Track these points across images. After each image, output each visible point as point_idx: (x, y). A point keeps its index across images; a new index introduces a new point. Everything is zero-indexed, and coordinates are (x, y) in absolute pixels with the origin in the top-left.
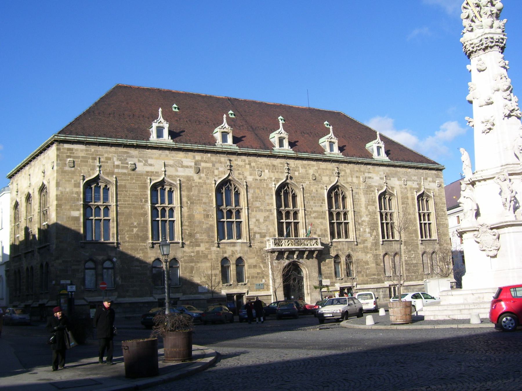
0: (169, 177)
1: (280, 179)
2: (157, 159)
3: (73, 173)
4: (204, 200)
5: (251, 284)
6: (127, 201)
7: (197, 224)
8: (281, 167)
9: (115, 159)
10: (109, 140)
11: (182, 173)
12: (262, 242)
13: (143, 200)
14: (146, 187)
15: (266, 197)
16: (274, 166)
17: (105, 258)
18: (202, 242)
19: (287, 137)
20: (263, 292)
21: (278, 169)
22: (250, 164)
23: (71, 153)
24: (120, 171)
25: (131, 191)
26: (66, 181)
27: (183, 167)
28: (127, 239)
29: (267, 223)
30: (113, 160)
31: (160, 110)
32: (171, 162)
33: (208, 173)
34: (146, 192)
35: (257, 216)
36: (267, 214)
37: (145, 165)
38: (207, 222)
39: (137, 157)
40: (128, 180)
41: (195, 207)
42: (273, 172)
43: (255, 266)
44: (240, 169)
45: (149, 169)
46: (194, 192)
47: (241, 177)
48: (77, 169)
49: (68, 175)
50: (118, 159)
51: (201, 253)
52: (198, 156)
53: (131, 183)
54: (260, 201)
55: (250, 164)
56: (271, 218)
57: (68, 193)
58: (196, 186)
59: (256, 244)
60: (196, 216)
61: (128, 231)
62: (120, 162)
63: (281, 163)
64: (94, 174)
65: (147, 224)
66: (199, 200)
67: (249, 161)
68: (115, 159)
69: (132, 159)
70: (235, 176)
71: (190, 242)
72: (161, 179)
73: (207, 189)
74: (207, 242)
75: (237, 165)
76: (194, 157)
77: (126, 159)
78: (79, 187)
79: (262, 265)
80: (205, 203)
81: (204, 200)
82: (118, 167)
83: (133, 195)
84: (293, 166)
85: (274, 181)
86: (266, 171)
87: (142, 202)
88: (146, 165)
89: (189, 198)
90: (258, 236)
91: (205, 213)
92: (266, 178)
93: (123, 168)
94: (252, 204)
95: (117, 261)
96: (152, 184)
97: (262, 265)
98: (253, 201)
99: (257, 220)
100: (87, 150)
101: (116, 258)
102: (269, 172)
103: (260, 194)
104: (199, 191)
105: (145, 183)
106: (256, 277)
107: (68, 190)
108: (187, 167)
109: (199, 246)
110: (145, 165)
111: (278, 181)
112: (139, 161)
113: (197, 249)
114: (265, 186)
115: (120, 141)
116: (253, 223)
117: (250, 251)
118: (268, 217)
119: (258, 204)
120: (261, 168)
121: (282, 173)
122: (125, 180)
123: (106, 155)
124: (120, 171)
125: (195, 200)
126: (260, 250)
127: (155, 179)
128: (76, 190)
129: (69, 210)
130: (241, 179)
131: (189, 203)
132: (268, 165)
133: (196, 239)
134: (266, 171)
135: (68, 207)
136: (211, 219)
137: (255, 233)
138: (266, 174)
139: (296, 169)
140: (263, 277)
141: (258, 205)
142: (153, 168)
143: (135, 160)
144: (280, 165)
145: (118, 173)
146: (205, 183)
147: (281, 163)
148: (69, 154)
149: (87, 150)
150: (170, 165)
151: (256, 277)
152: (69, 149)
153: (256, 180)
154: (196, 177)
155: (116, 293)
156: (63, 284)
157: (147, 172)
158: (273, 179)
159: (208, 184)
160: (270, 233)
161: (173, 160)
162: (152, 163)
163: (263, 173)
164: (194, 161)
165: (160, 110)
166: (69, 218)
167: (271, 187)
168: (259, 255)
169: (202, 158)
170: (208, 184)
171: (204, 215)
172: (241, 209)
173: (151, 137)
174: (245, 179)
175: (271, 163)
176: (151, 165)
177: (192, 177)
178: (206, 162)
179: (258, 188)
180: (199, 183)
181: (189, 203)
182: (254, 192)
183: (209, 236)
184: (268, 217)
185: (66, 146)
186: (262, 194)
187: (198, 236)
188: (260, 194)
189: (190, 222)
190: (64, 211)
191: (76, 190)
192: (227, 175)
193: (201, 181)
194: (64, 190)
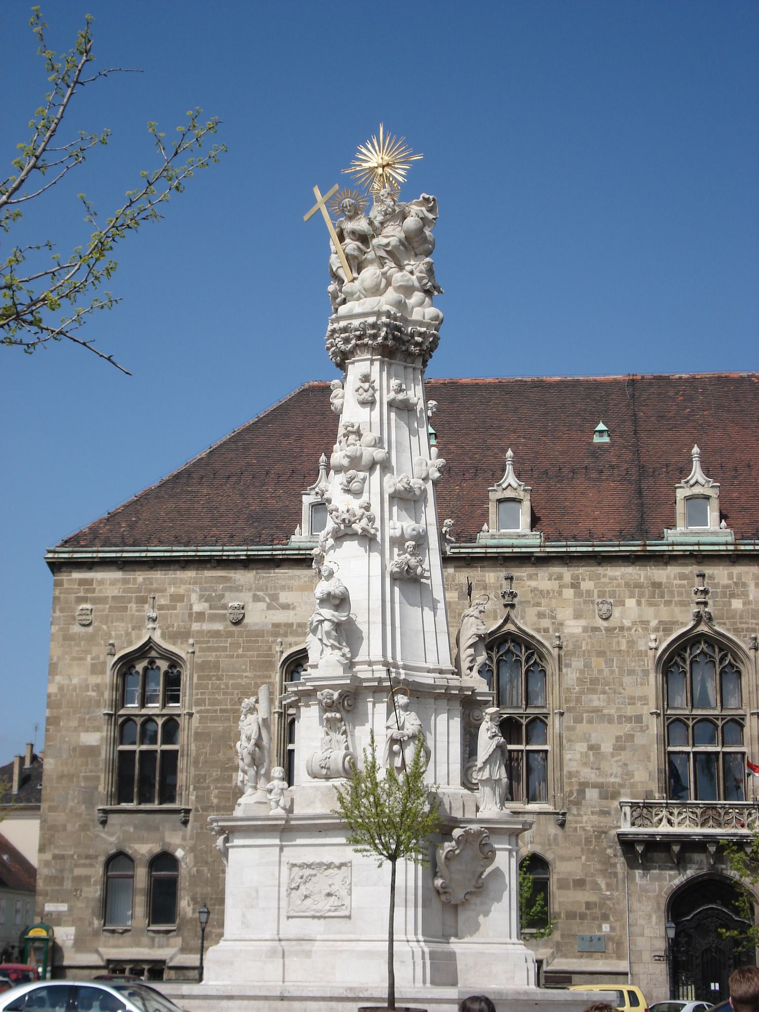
1: (675, 623)
3: (91, 639)
5: (563, 936)
6: (219, 703)
8: (680, 586)
9: (194, 597)
10: (179, 552)
12: (605, 813)
14: (270, 665)
15: (627, 680)
16: (657, 585)
17: (157, 849)
19: (713, 493)
20: (601, 962)
21: (671, 593)
22: (575, 585)
23: (87, 591)
24: (206, 626)
25: (232, 677)
26: (73, 659)
28: (215, 801)
29: (624, 756)
30: (189, 600)
34: (270, 677)
35: (593, 735)
36: (627, 727)
37: (269, 607)
39: (250, 590)
40: (224, 649)
42: (651, 604)
43: (580, 884)
44: (543, 601)
45: (280, 617)
47: (546, 623)
48: (98, 629)
49: (78, 645)
50: (201, 597)
53: (232, 657)
54: (604, 693)
55: (575, 585)
56: (640, 740)
57: (75, 689)
59: (585, 818)
61: (217, 780)
62: (206, 605)
63: (682, 577)
64: (139, 637)
67: (575, 578)
68: (194, 597)
69: (237, 594)
70: (527, 622)
75: (534, 590)
78: (103, 672)
79: (602, 882)
82: (200, 616)
83: (236, 686)
84: (725, 581)
85: (656, 630)
86: (631, 603)
88: (275, 608)
90: (592, 794)
92: (627, 623)
93: (213, 618)
94: (578, 700)
95: (184, 858)
96: (285, 655)
97: (602, 882)
98: (582, 692)
99: (591, 748)
100: (125, 581)
101: (184, 848)
102: (639, 603)
103: (606, 672)
105: (268, 656)
106: (583, 917)
107: (75, 681)
111: (667, 631)
112: (256, 599)
114: (624, 647)
115: (205, 551)
116: (578, 756)
117: (566, 838)
118: (630, 737)
119: (596, 701)
120: (613, 594)
121: (682, 604)
122: (216, 649)
123: (172, 590)
124: (206, 626)
126: (598, 837)
127: (296, 644)
128: (95, 680)
129: (76, 729)
130: (546, 630)
132: (638, 585)
134: (631, 603)
135: (74, 723)
137: (583, 786)
138: (629, 611)
139: (737, 589)
140: (605, 918)
141: (596, 703)
142: (291, 613)
143: (245, 597)
144: (678, 582)
145: (200, 632)
147: (682, 577)
148: (81, 594)
149: (125, 581)
151: (583, 917)
152: (82, 582)
153: (596, 629)
155: (179, 941)
156: (50, 913)
157: (276, 626)
158: (654, 623)
160: (633, 786)
162: (289, 601)
163: (617, 612)
166: (74, 749)
167: (643, 648)
168: (593, 852)
172: (546, 716)
173: (297, 530)
174: (557, 630)
175: (646, 577)
176: (286, 607)
179: (601, 654)
182: (587, 666)
184: (630, 737)
185: (77, 575)
186: (612, 672)
188: (606, 672)
190: (64, 732)
191: (95, 680)
192: (501, 621)
194: (67, 682)
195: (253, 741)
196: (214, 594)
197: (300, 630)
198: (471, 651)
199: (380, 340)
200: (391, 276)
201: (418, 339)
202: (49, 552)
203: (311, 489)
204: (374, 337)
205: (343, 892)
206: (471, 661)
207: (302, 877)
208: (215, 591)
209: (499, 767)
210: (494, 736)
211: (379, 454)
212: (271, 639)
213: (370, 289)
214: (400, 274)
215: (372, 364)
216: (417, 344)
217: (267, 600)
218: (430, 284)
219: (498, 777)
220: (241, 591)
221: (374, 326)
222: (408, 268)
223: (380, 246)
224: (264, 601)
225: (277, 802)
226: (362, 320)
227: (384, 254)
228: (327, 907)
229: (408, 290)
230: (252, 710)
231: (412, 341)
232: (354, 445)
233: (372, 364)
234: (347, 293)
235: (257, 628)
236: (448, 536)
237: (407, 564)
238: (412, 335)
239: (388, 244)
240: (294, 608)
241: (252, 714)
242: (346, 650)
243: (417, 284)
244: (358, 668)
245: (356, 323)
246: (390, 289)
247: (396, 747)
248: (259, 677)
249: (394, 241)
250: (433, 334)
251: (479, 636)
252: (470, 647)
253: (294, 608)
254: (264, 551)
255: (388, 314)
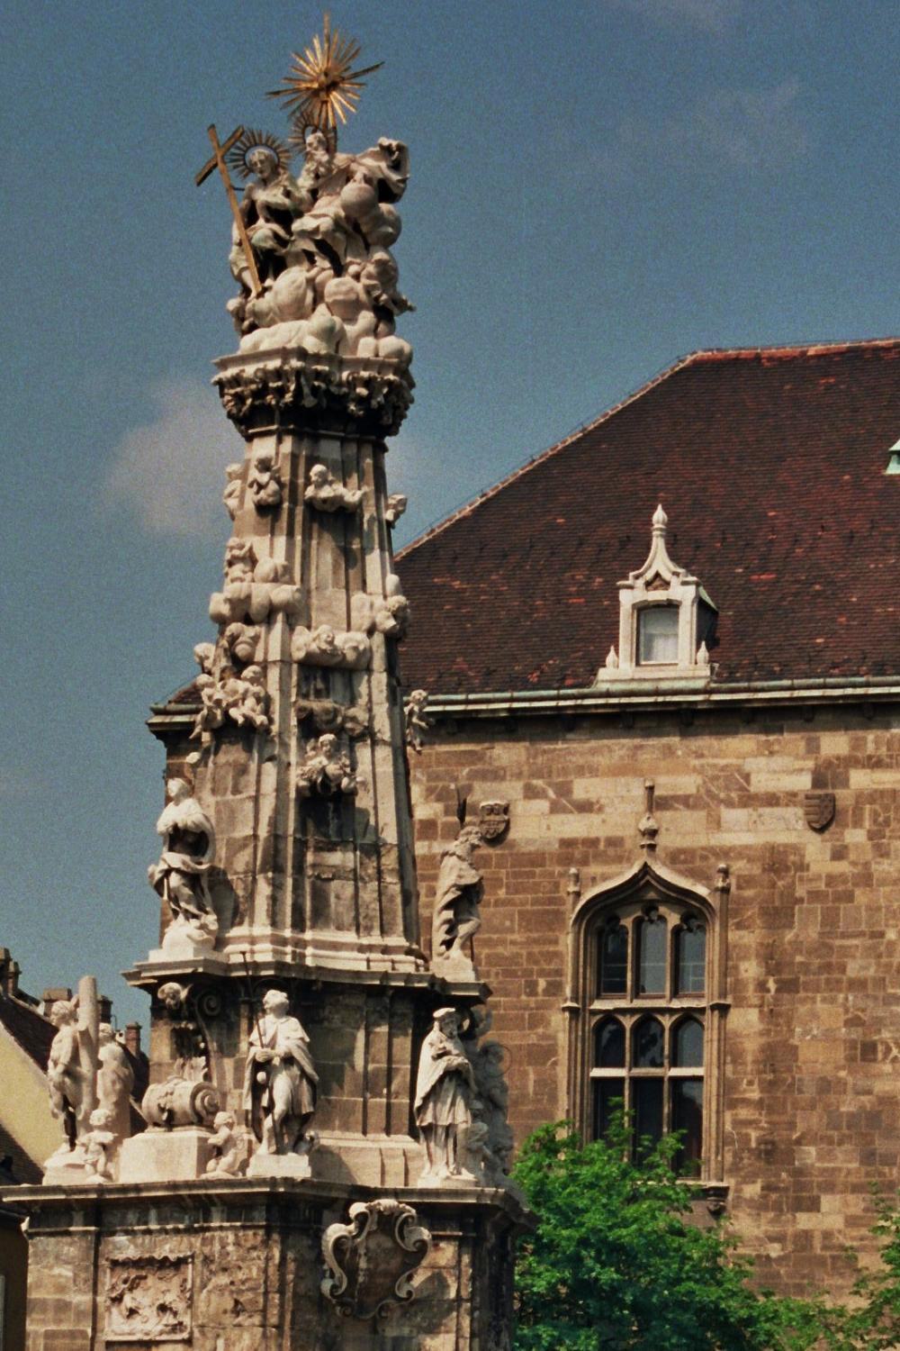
0: (674, 858)
2: (618, 771)
4: (853, 969)
7: (810, 1092)
11: (742, 831)
13: (542, 983)
14: (558, 916)
18: (830, 1188)
27: (749, 800)
31: (659, 516)
32: (688, 784)
33: (887, 822)
34: (556, 942)
37: (555, 809)
38: (863, 1083)
39: (519, 775)
41: (803, 1009)
45: (575, 826)
46: (805, 930)
50: (430, 791)
51: (817, 1244)
52: (835, 743)
58: (815, 896)
60: (805, 1053)
62: (439, 807)
65: (553, 1099)
66: (828, 967)
69: (495, 785)
71: (767, 1188)
72: (635, 869)
73: (873, 909)
74: (856, 1189)
76: (813, 748)
77: (469, 789)
80: (858, 985)
81: (853, 969)
87: (533, 993)
88: (564, 810)
89: (772, 959)
91: (856, 1034)
104: (830, 920)
108: (772, 800)
109: (814, 1206)
110: (555, 809)
112: (531, 793)
113: (805, 1221)
125: (805, 967)
127: (605, 878)
131: (772, 985)
133: (799, 1173)
136: (887, 1068)
142: (595, 819)
143: (511, 791)
146: (866, 879)
150: (687, 802)
154: (816, 849)
157: (567, 843)
159: (883, 883)
161: (699, 771)
162: (593, 796)
164: (810, 764)
165: (659, 516)
169: (857, 745)
170: (883, 883)
171: (852, 1045)
176: (585, 807)
177: (796, 849)
178: (875, 763)
180: (831, 879)
181: (772, 985)
183: (868, 1157)
187: (810, 1155)
189: (769, 1087)
193: (842, 867)
195: (60, 1068)
196: (453, 786)
197: (611, 851)
198: (449, 914)
199: (288, 398)
200: (323, 284)
201: (362, 391)
202: (158, 712)
203: (637, 577)
204: (281, 392)
205: (180, 1306)
206: (448, 932)
207: (125, 1282)
208: (455, 779)
209: (453, 1104)
210: (440, 1056)
211: (283, 593)
212: (558, 869)
213: (289, 306)
214: (337, 280)
215: (280, 441)
216: (361, 401)
217: (551, 794)
218: (384, 297)
219: (449, 1121)
220: (503, 779)
221: (278, 374)
222: (353, 269)
223: (305, 234)
224: (545, 796)
225: (94, 1165)
226: (261, 365)
227: (311, 247)
228: (160, 1327)
229: (350, 309)
230: (71, 1017)
231: (352, 396)
232: (242, 580)
233: (280, 441)
234: (255, 314)
235: (532, 849)
236: (415, 720)
237: (323, 771)
238: (352, 384)
239: (316, 230)
240: (601, 810)
241: (68, 1023)
242: (211, 920)
243: (363, 297)
244: (229, 949)
245: (250, 370)
246: (322, 308)
247: (261, 1076)
248: (536, 941)
249: (325, 224)
250: (389, 383)
251: (459, 887)
252: (448, 907)
253: (601, 810)
254: (544, 700)
255: (302, 353)
